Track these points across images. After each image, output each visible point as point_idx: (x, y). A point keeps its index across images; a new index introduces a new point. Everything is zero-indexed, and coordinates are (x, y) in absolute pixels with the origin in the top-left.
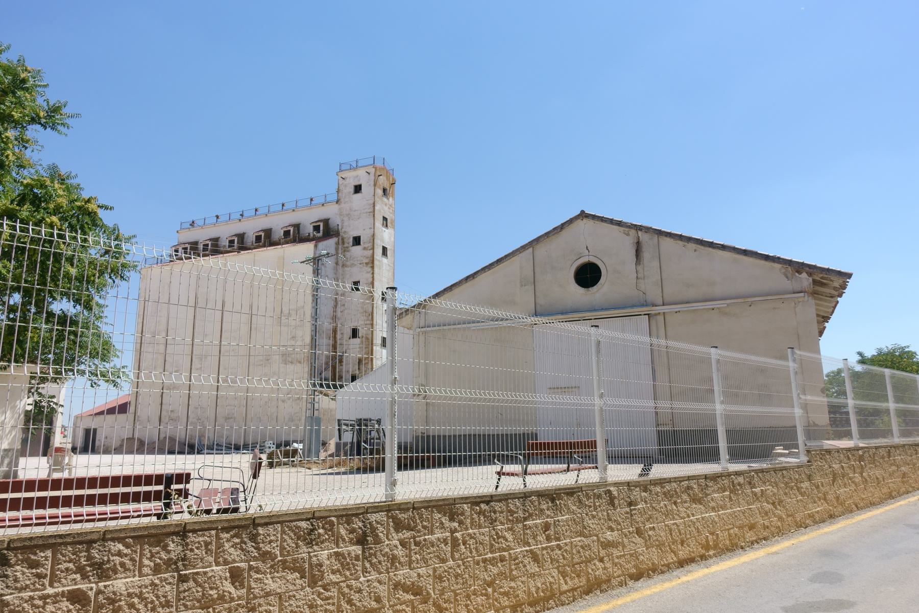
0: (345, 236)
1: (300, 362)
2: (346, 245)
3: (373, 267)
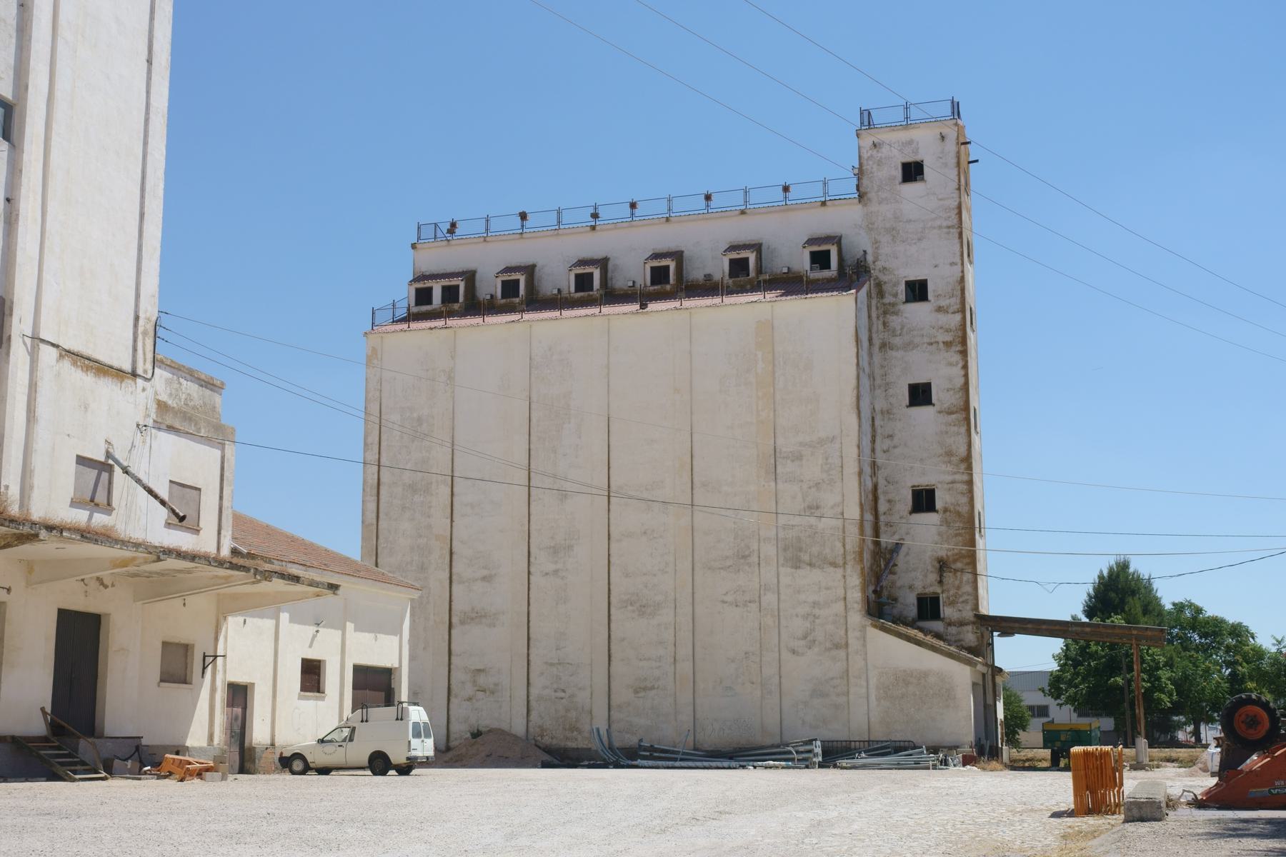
0: (884, 278)
1: (834, 565)
2: (888, 299)
3: (964, 353)
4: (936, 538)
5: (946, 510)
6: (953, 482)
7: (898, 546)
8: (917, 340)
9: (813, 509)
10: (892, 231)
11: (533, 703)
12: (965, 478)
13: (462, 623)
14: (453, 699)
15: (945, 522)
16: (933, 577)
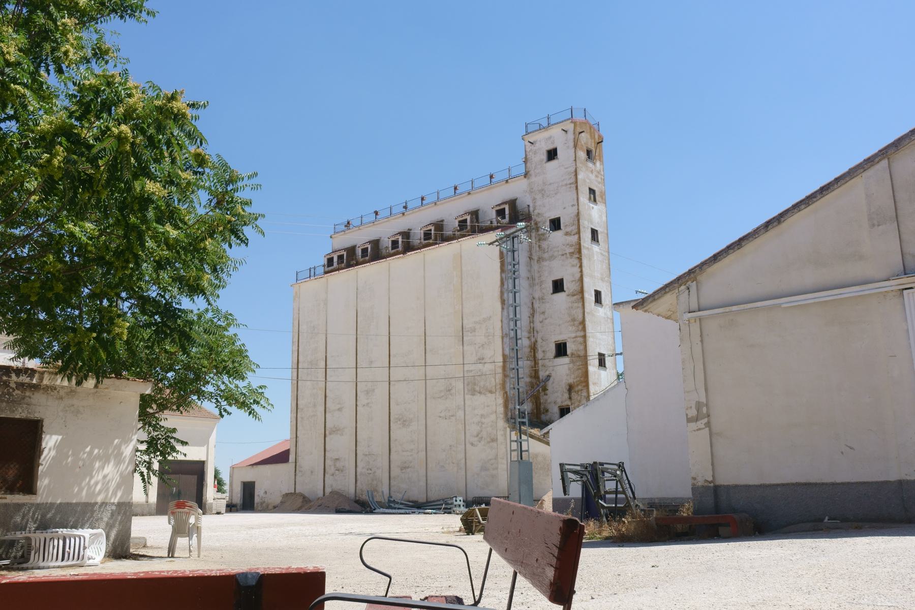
0: (538, 220)
1: (491, 392)
2: (541, 231)
3: (580, 259)
4: (568, 372)
5: (572, 354)
6: (576, 337)
7: (549, 376)
8: (556, 254)
9: (481, 360)
10: (542, 191)
11: (358, 477)
12: (582, 334)
13: (330, 434)
14: (327, 475)
15: (572, 362)
16: (566, 395)
